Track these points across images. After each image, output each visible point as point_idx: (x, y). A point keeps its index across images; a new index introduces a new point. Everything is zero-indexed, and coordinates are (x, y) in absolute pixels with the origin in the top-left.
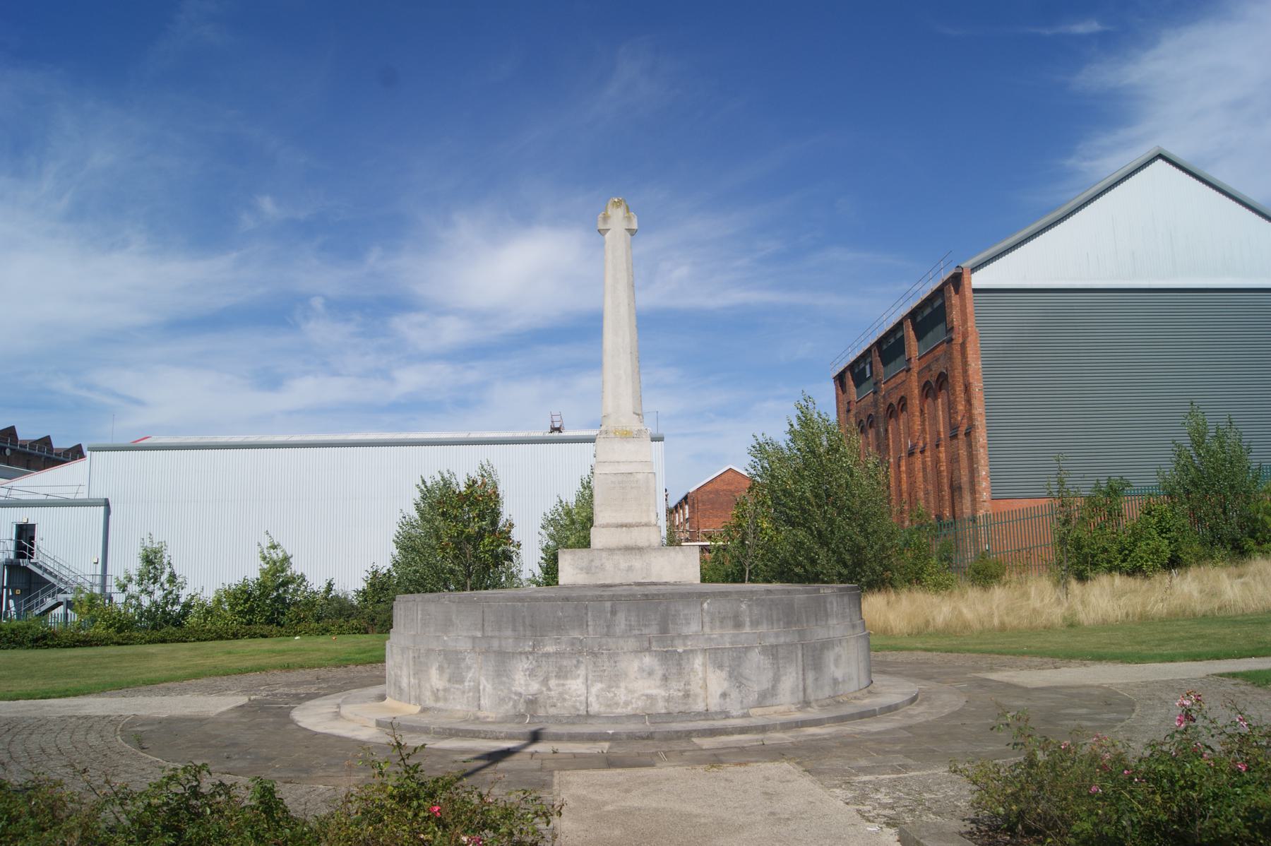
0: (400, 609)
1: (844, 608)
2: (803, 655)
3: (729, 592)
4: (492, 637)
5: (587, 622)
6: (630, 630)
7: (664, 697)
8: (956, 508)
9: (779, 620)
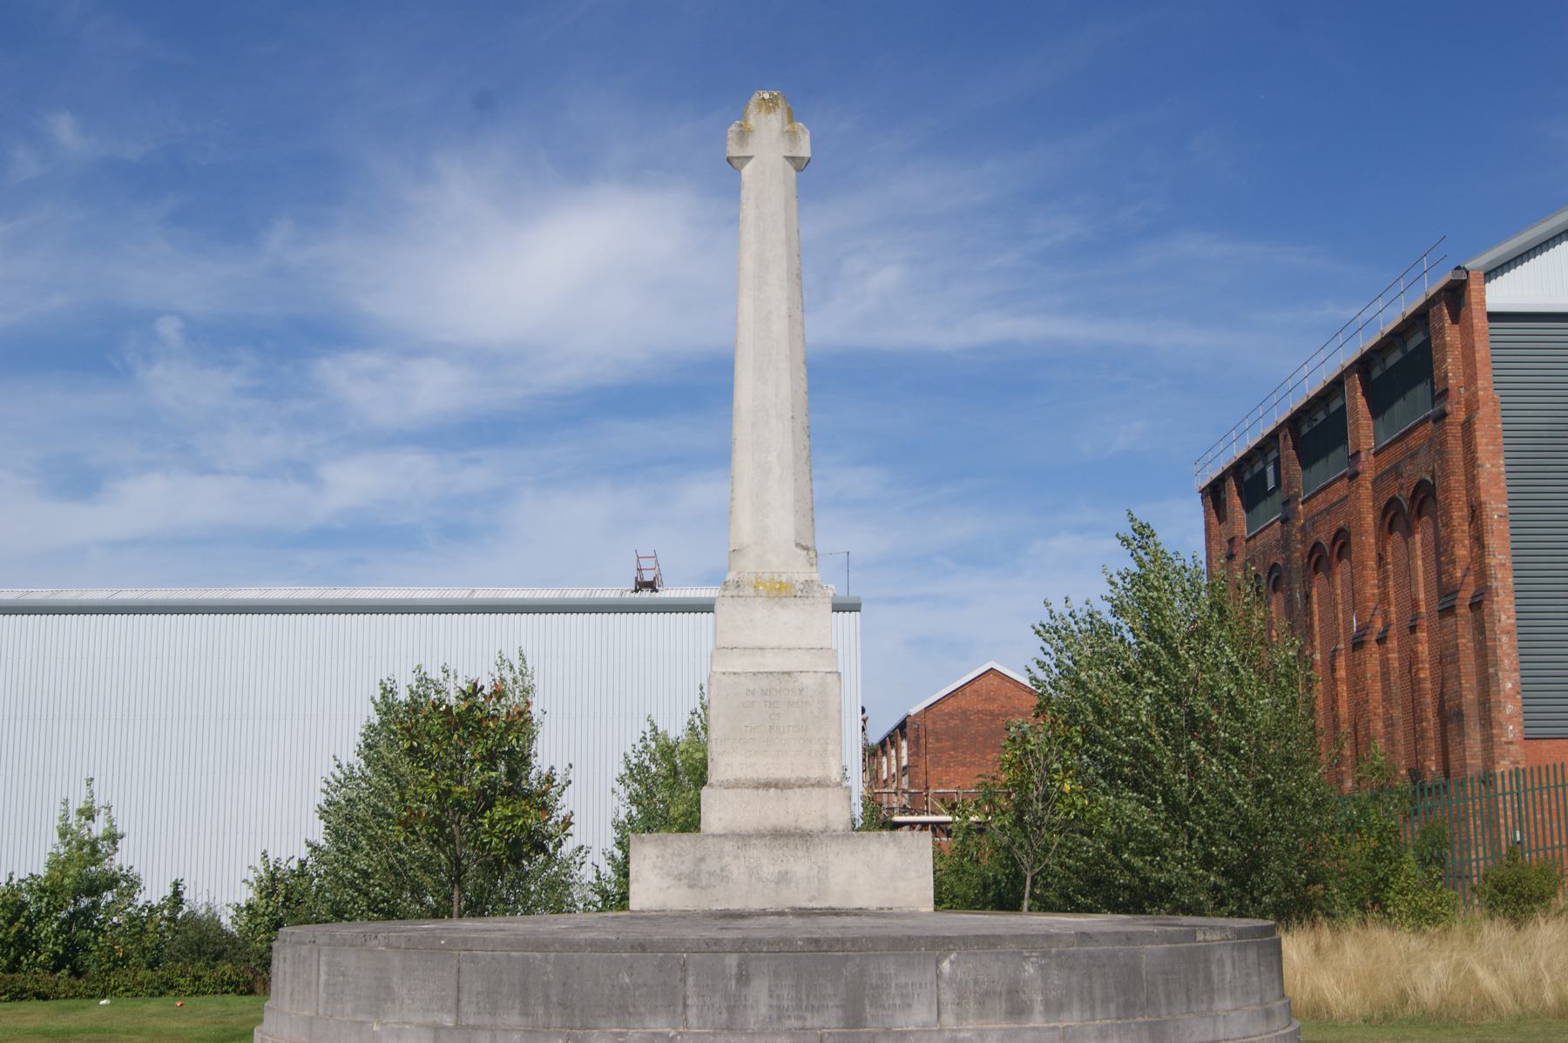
0: (285, 959)
1: (1248, 975)
3: (1000, 936)
4: (476, 1028)
5: (685, 998)
6: (780, 1018)
8: (1451, 756)
9: (1106, 1000)
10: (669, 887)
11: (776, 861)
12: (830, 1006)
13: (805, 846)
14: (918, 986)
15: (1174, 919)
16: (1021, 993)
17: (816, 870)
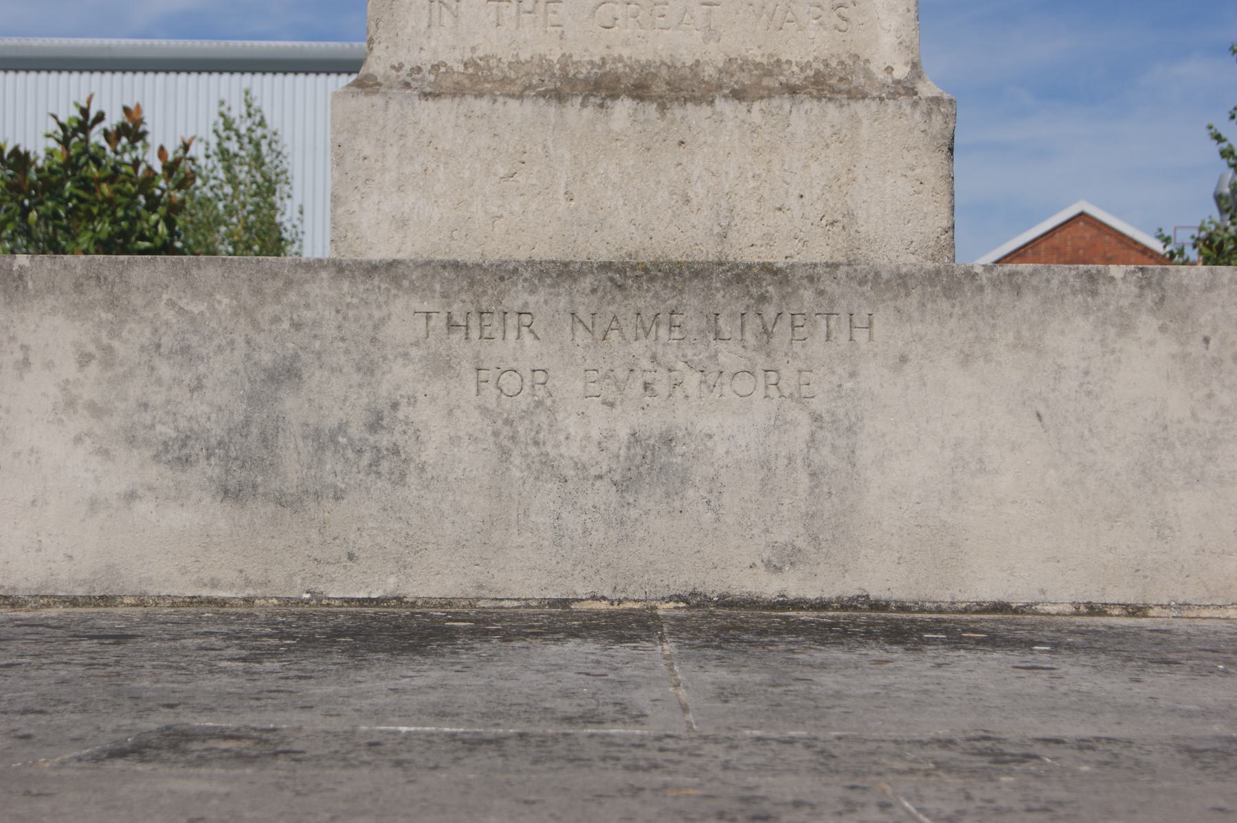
10: (131, 496)
11: (620, 387)
13: (753, 323)
17: (804, 430)
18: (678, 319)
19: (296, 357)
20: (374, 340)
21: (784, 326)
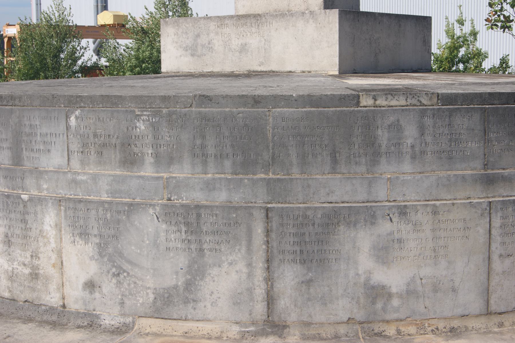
2: (268, 232)
3: (121, 96)
7: (7, 271)
9: (220, 157)
10: (181, 56)
12: (4, 148)
14: (54, 135)
15: (445, 86)
16: (133, 146)
18: (247, 24)
19: (199, 33)
20: (209, 30)
21: (261, 24)
